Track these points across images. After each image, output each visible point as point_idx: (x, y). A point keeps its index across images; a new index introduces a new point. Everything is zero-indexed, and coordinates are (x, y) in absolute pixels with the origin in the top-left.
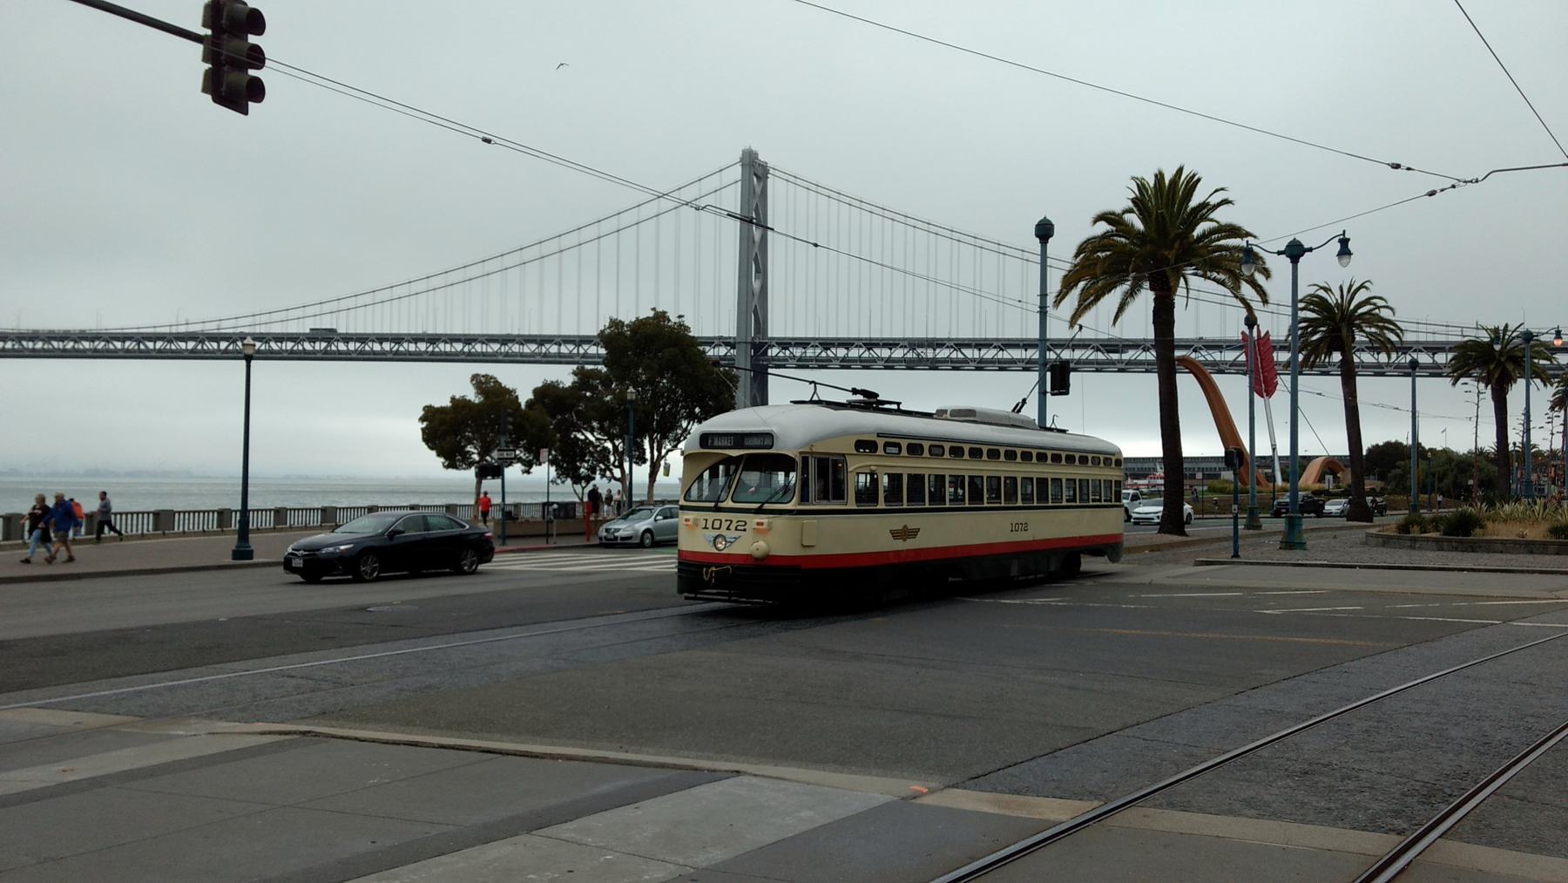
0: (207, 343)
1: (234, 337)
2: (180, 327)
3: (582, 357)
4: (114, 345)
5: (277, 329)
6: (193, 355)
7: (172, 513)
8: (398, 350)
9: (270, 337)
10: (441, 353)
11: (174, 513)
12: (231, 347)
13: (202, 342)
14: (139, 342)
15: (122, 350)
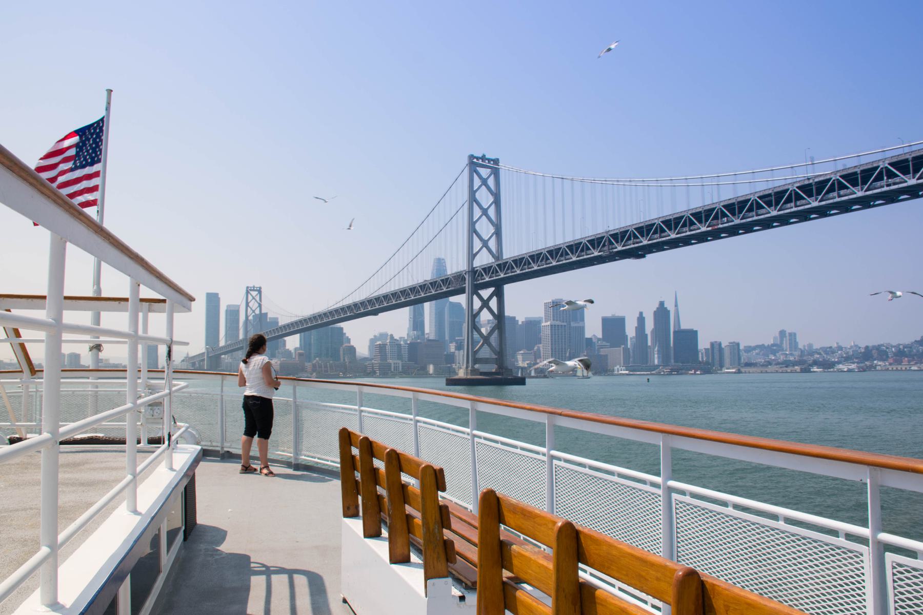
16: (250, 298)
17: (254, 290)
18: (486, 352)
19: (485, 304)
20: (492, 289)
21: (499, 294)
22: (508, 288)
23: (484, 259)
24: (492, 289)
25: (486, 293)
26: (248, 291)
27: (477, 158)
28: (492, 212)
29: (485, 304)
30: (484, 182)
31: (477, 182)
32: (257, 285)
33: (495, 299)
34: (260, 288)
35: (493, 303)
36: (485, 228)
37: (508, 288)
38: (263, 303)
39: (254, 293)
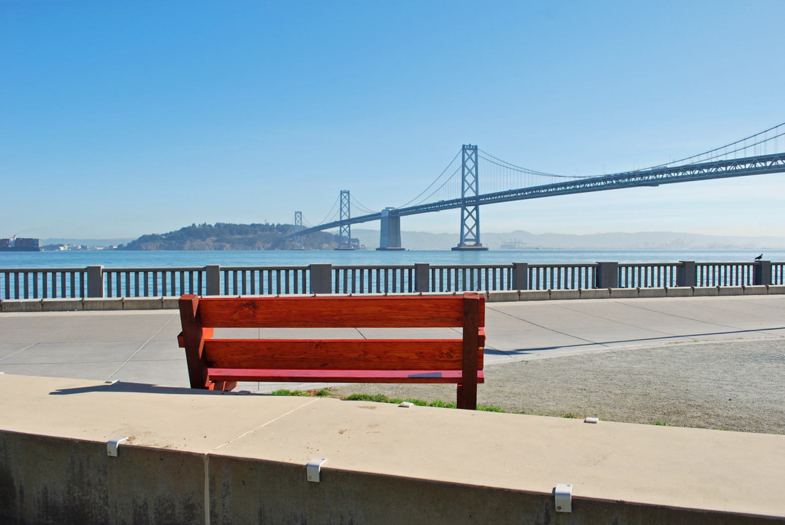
0: (738, 166)
1: (754, 159)
2: (713, 159)
3: (728, 173)
4: (703, 171)
5: (740, 155)
6: (693, 178)
7: (694, 265)
8: (662, 177)
9: (756, 159)
10: (739, 170)
11: (696, 265)
12: (774, 164)
13: (755, 163)
14: (642, 177)
15: (707, 173)
16: (343, 197)
17: (345, 193)
18: (470, 236)
19: (470, 214)
20: (474, 207)
21: (477, 209)
22: (481, 207)
23: (470, 194)
24: (474, 207)
25: (470, 208)
26: (342, 193)
27: (467, 146)
28: (474, 171)
29: (470, 214)
30: (470, 157)
31: (466, 157)
32: (347, 190)
33: (475, 211)
34: (349, 191)
35: (474, 214)
36: (470, 179)
37: (480, 207)
38: (351, 201)
39: (345, 194)
